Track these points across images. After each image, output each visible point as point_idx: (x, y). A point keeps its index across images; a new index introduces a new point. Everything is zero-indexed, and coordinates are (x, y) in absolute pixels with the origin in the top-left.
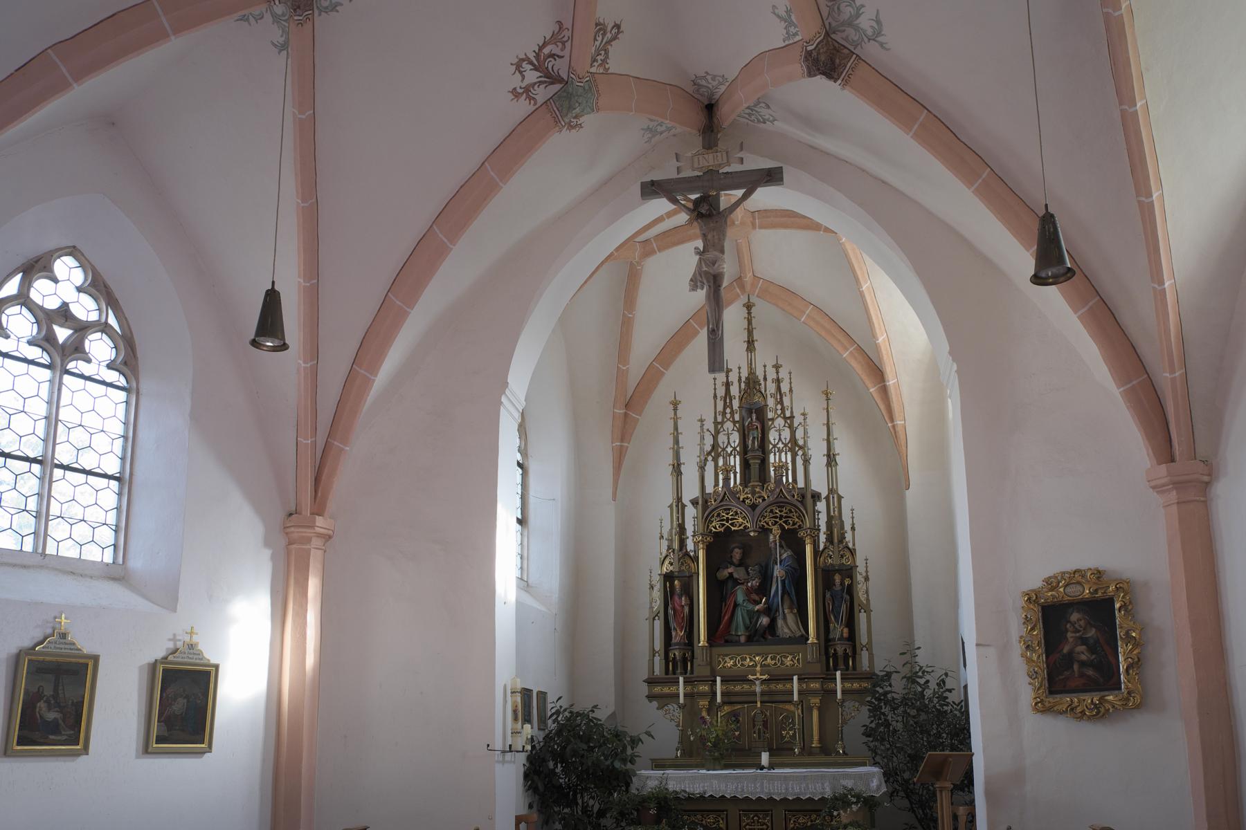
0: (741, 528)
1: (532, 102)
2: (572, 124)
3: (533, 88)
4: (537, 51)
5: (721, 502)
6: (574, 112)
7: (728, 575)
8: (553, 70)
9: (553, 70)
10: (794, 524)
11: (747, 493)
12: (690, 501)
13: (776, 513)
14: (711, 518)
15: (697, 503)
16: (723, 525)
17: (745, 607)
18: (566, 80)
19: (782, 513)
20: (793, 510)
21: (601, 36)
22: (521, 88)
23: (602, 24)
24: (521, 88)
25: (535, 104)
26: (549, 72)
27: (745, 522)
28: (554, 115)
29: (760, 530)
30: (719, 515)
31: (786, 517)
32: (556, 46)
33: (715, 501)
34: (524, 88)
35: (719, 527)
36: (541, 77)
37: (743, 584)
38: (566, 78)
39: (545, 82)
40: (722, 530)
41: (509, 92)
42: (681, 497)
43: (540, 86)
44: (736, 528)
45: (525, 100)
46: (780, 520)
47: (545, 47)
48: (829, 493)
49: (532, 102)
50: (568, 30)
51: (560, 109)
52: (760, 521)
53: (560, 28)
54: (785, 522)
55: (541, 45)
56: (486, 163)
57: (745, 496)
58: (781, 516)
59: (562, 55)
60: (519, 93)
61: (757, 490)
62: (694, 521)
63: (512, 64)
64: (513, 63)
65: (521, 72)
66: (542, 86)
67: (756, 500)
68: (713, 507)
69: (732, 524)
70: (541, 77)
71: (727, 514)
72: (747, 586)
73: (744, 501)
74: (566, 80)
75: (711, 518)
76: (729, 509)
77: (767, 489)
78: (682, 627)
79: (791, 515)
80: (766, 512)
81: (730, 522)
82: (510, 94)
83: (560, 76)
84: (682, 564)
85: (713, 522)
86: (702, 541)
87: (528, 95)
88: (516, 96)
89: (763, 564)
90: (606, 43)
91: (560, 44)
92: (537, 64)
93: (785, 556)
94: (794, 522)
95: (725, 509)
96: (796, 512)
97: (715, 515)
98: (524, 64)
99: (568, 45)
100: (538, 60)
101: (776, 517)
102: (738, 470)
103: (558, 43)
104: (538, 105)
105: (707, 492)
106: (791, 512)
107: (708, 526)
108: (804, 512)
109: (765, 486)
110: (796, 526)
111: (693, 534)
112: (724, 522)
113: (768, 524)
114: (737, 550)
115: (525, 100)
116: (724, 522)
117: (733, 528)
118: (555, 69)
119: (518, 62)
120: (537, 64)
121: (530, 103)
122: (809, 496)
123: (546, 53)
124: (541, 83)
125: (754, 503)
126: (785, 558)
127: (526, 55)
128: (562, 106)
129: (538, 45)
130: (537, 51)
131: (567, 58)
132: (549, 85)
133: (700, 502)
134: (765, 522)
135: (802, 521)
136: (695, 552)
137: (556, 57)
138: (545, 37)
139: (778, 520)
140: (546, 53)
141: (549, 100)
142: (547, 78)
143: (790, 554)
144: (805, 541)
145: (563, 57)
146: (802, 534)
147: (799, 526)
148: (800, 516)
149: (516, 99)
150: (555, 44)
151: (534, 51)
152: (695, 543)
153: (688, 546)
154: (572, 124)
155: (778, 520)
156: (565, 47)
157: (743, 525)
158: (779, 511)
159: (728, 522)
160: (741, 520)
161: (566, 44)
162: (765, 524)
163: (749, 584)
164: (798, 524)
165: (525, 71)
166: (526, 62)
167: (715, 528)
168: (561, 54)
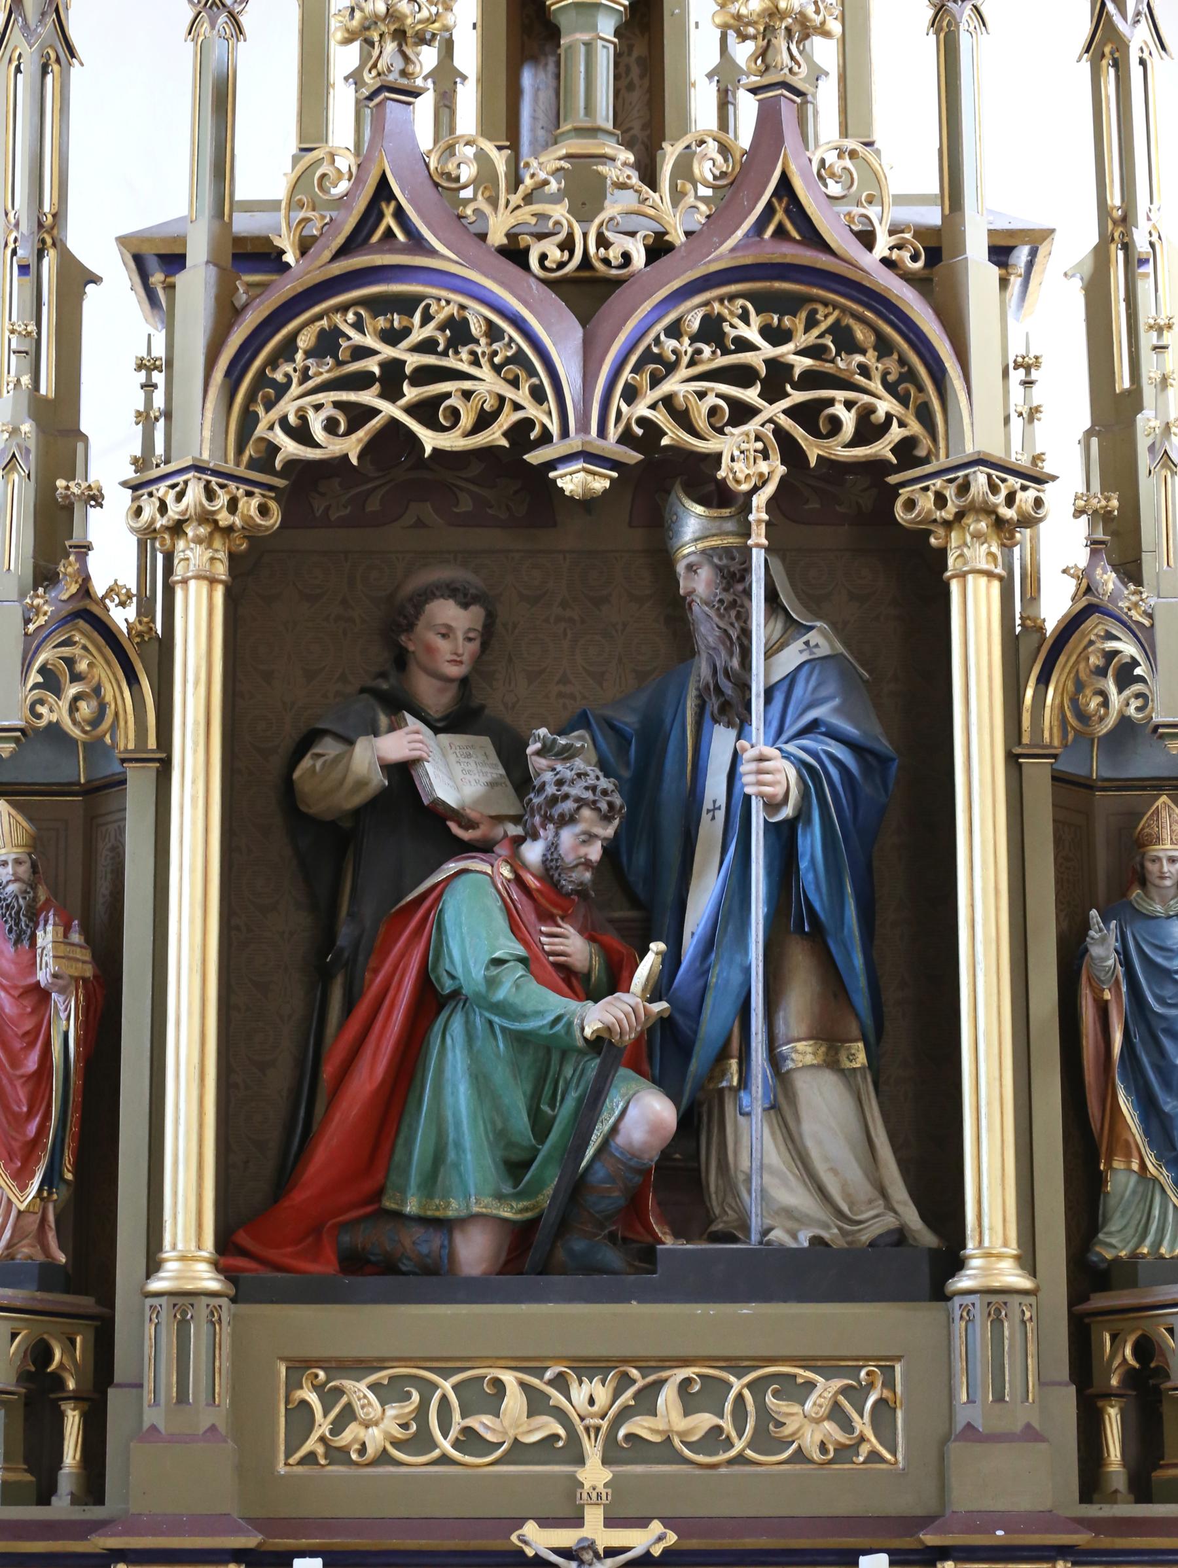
0: (495, 435)
5: (343, 251)
7: (379, 780)
10: (868, 430)
11: (528, 199)
12: (123, 241)
13: (744, 345)
14: (273, 362)
15: (174, 261)
16: (359, 415)
17: (501, 1008)
19: (786, 351)
20: (861, 334)
27: (523, 396)
29: (633, 457)
30: (328, 344)
31: (810, 380)
33: (304, 247)
35: (331, 426)
37: (484, 848)
40: (351, 446)
42: (59, 216)
44: (452, 441)
46: (772, 393)
48: (1105, 240)
52: (631, 394)
54: (805, 414)
57: (525, 214)
58: (778, 368)
61: (611, 172)
62: (148, 386)
67: (603, 242)
68: (286, 288)
69: (426, 411)
71: (392, 337)
72: (515, 861)
73: (514, 253)
75: (273, 362)
76: (407, 304)
77: (684, 169)
78: (35, 1144)
79: (846, 364)
80: (674, 331)
81: (411, 393)
84: (51, 682)
85: (282, 389)
86: (206, 518)
89: (629, 720)
93: (791, 657)
94: (866, 413)
95: (378, 305)
96: (884, 347)
97: (305, 341)
101: (742, 376)
102: (467, 57)
105: (239, 196)
106: (847, 344)
107: (249, 421)
108: (944, 350)
109: (670, 153)
110: (882, 448)
111: (129, 473)
112: (368, 397)
113: (683, 418)
114: (446, 611)
116: (368, 397)
117: (430, 440)
122: (976, 248)
125: (586, 261)
126: (792, 678)
133: (198, 252)
134: (668, 401)
135: (924, 415)
136: (145, 609)
139: (751, 395)
143: (824, 650)
144: (942, 553)
146: (926, 502)
147: (905, 448)
148: (910, 375)
152: (147, 537)
153: (92, 559)
155: (751, 395)
157: (507, 419)
158: (769, 333)
159: (392, 393)
160: (488, 384)
162: (660, 417)
163: (533, 852)
164: (896, 433)
167: (301, 434)
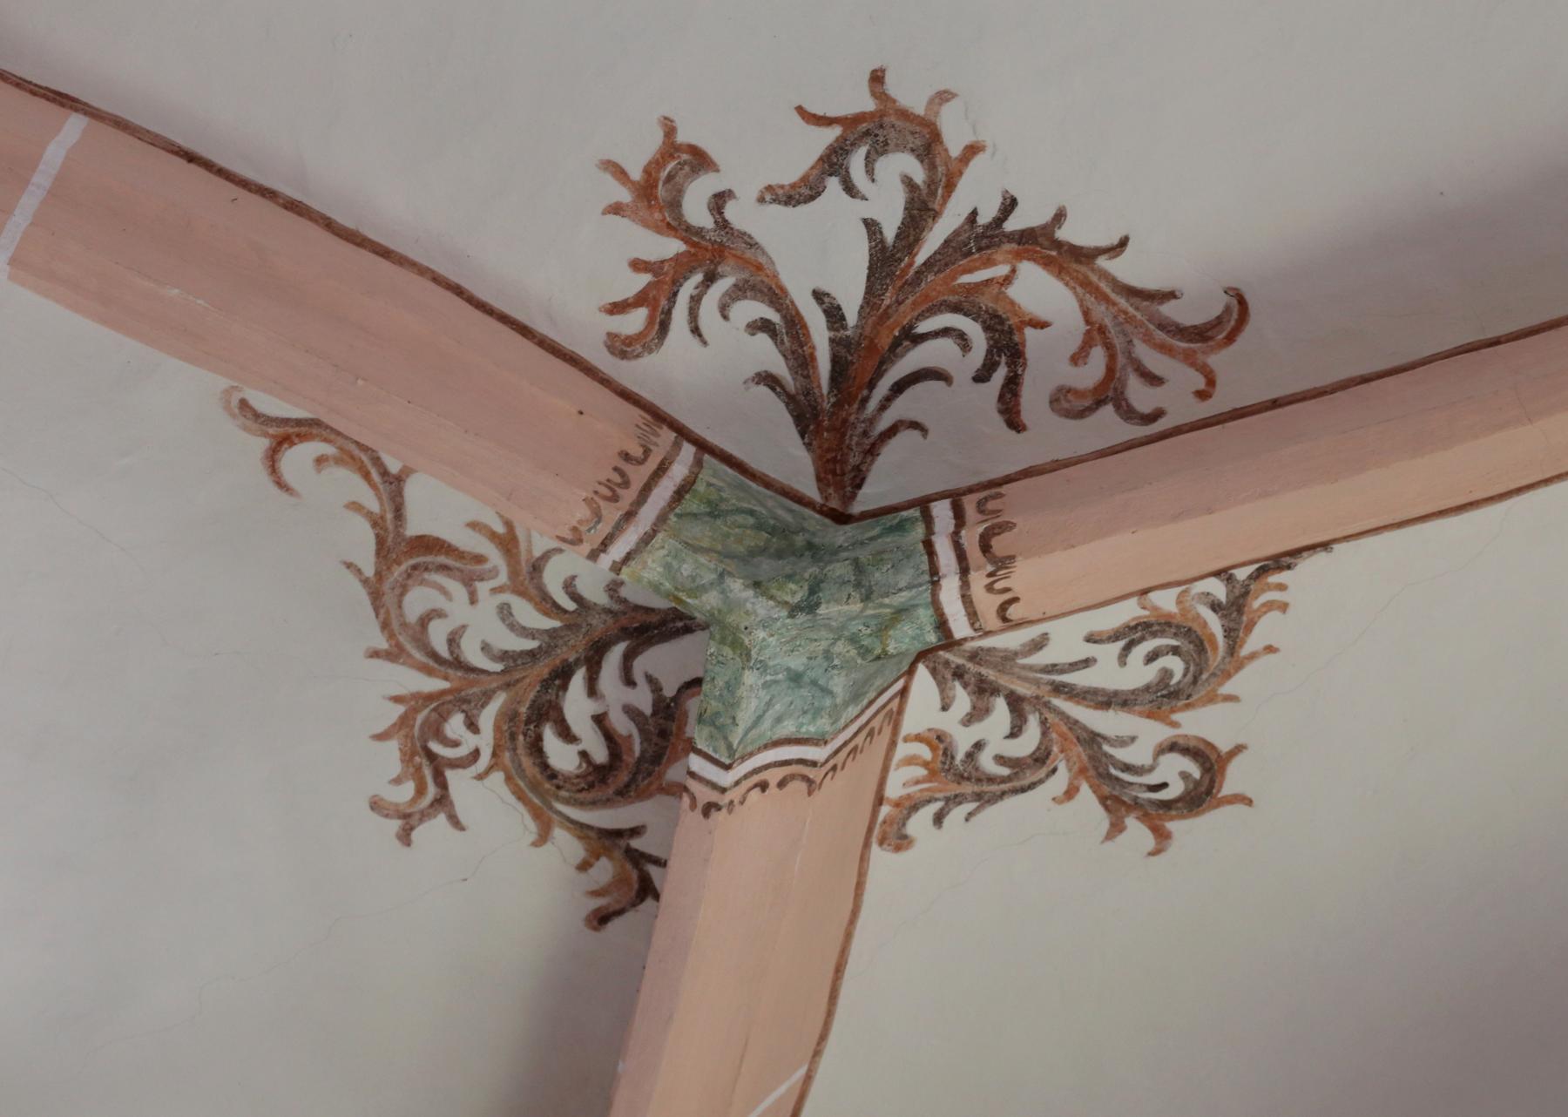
1: (635, 321)
2: (455, 726)
3: (740, 291)
4: (1011, 225)
6: (736, 586)
8: (899, 388)
9: (899, 388)
18: (857, 508)
21: (1149, 674)
22: (719, 201)
23: (1232, 650)
24: (719, 201)
25: (622, 347)
26: (879, 373)
28: (639, 475)
32: (1075, 343)
34: (723, 225)
36: (834, 315)
38: (872, 495)
39: (802, 361)
41: (670, 130)
43: (763, 339)
45: (638, 265)
47: (1047, 263)
49: (635, 321)
50: (1202, 395)
51: (691, 504)
53: (1201, 333)
55: (1062, 234)
56: (75, 126)
59: (1026, 416)
60: (675, 205)
63: (877, 78)
64: (892, 86)
65: (833, 163)
66: (767, 355)
70: (834, 315)
74: (857, 508)
82: (652, 142)
83: (872, 451)
87: (678, 270)
88: (646, 190)
90: (1092, 739)
91: (1092, 372)
92: (922, 256)
98: (901, 165)
99: (1107, 426)
100: (954, 251)
103: (1098, 356)
104: (626, 372)
115: (638, 265)
118: (904, 407)
119: (905, 114)
120: (921, 258)
121: (617, 308)
123: (1013, 292)
124: (790, 333)
127: (972, 150)
128: (715, 511)
129: (1060, 217)
130: (1012, 224)
131: (1013, 452)
132: (790, 400)
137: (1000, 374)
138: (1124, 243)
140: (1013, 292)
141: (683, 433)
142: (835, 360)
145: (1015, 424)
149: (624, 195)
150: (1095, 333)
151: (1009, 205)
154: (455, 726)
156: (1081, 414)
161: (1108, 410)
165: (850, 189)
166: (919, 175)
168: (1033, 399)
